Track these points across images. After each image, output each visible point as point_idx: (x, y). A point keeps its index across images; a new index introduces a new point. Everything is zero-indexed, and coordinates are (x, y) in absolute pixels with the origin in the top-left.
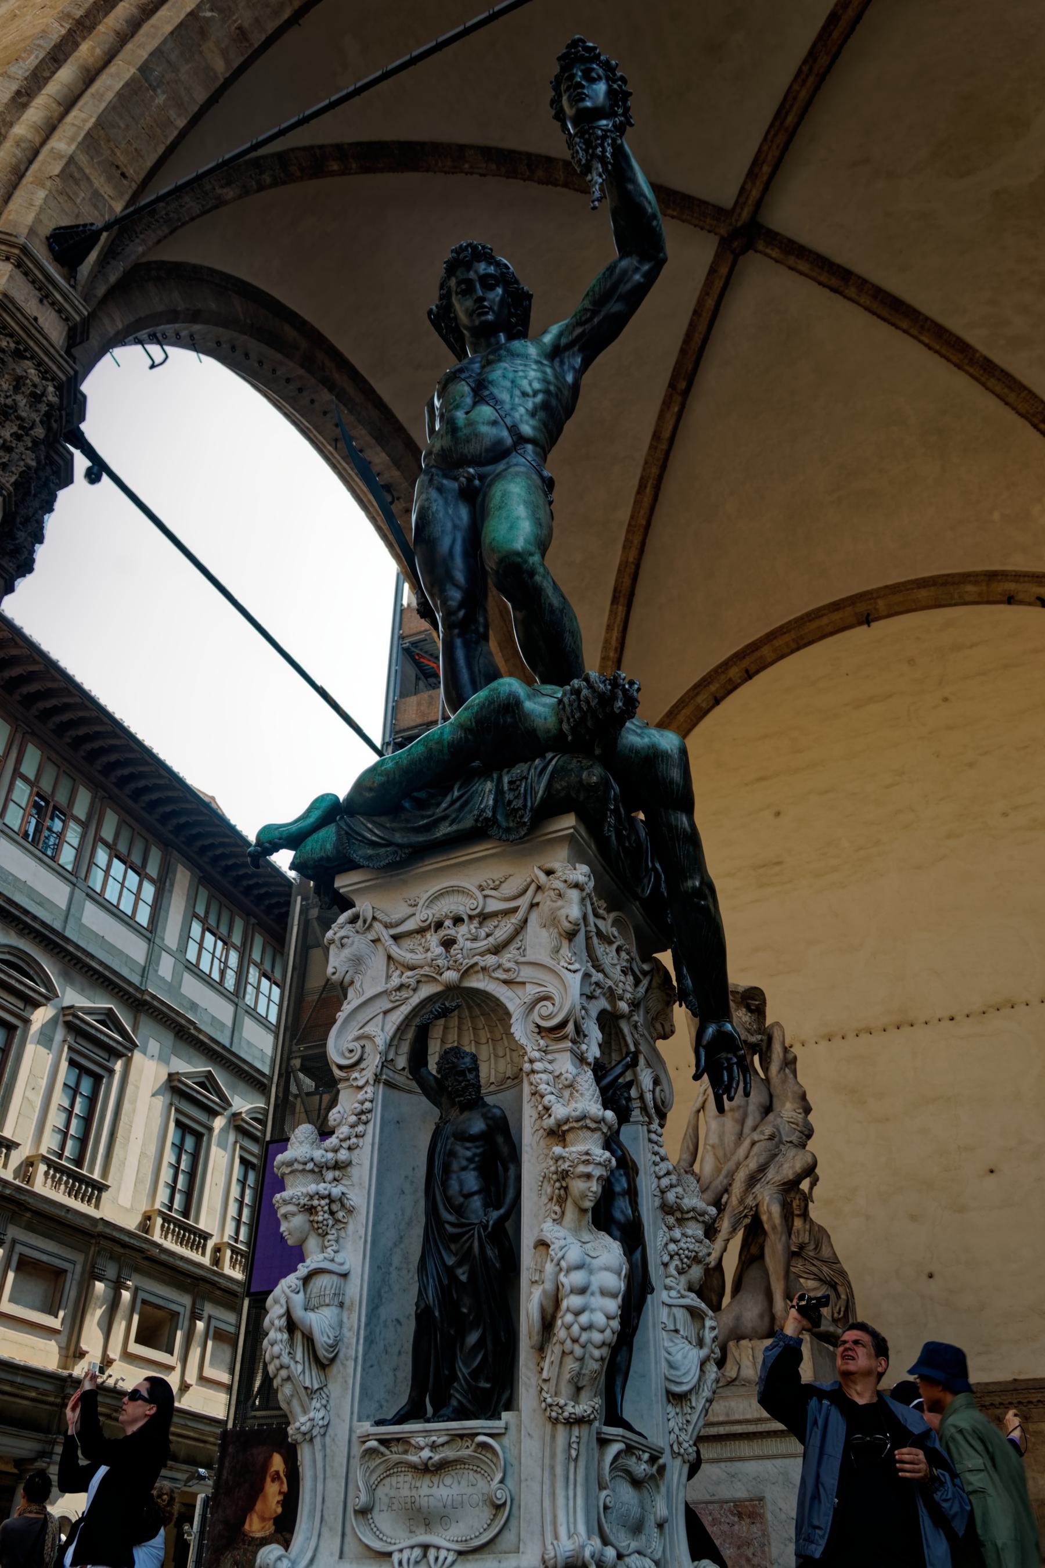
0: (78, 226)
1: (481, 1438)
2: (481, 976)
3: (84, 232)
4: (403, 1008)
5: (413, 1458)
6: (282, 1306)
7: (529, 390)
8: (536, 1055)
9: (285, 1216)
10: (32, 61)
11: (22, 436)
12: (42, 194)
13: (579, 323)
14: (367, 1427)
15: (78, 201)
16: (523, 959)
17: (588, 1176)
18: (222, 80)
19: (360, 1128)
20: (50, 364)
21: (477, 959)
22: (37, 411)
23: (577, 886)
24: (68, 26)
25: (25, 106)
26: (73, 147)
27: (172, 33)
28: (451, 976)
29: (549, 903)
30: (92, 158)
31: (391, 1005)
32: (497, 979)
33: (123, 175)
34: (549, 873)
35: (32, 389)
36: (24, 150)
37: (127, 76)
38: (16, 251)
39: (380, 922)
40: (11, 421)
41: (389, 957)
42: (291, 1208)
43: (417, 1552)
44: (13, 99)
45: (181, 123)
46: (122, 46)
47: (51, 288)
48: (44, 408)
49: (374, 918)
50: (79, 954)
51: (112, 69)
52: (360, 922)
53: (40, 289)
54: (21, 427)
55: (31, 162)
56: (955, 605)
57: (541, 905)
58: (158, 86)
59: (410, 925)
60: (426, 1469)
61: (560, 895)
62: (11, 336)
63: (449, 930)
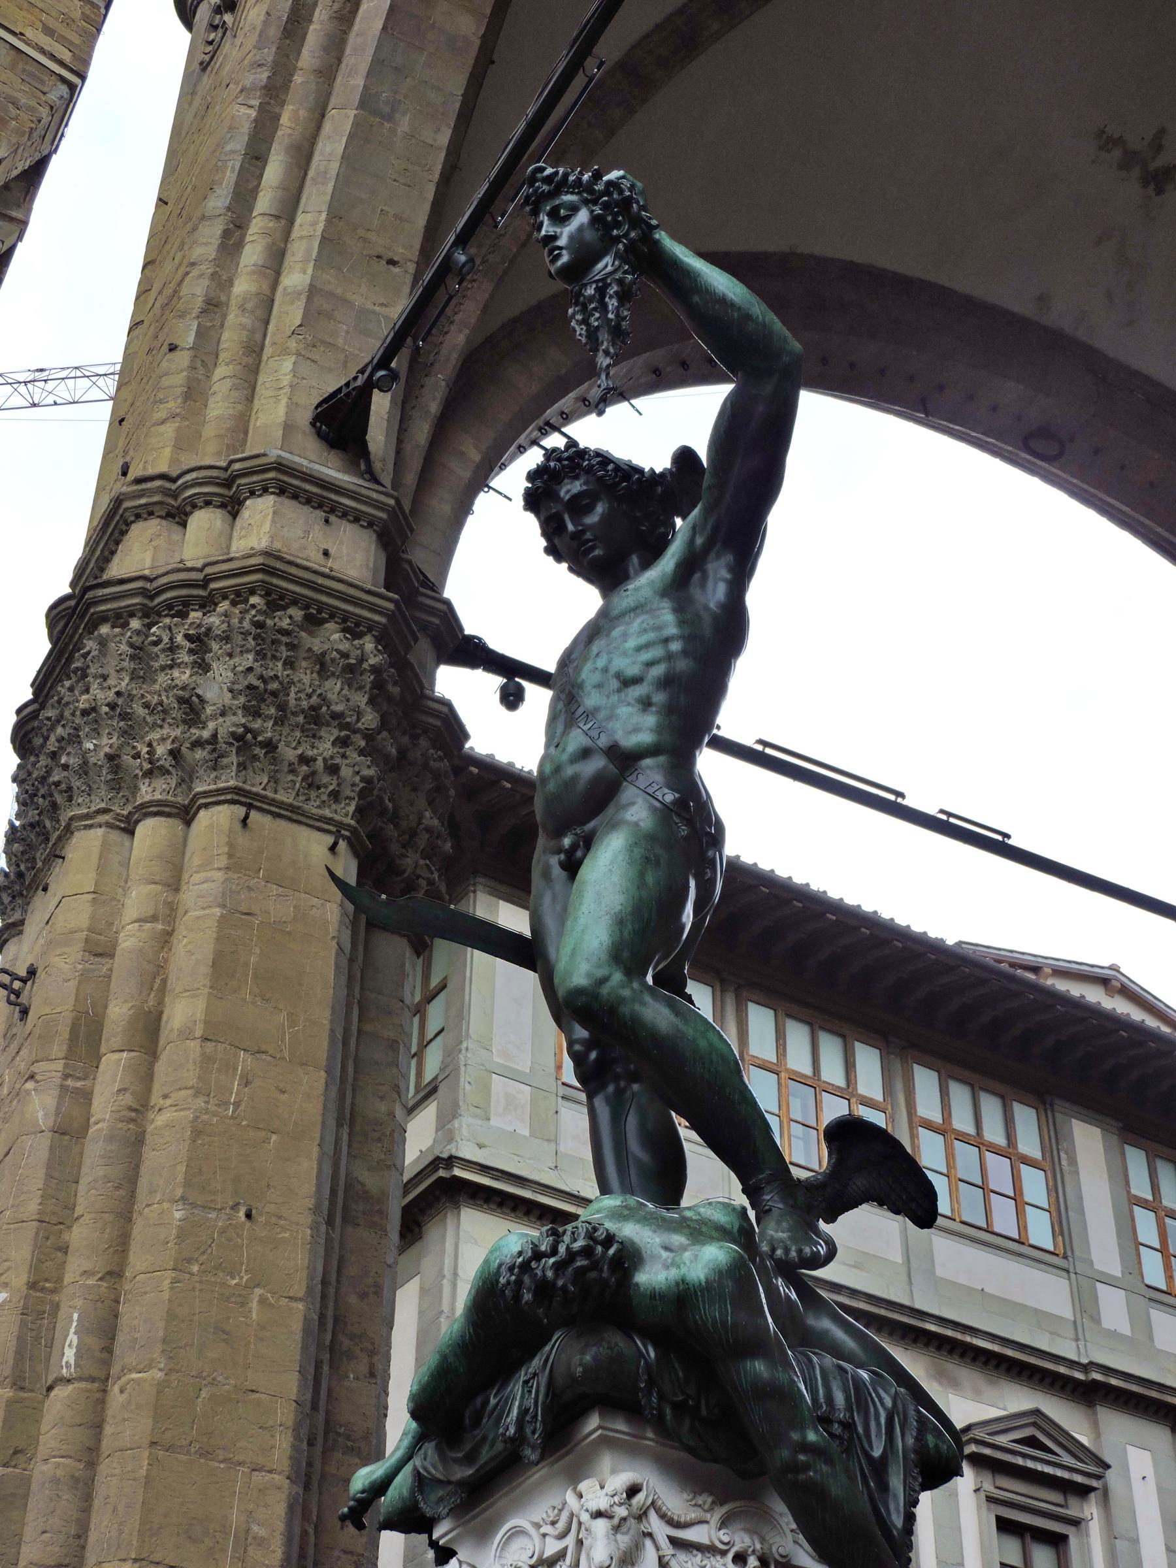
0: (339, 390)
3: (348, 395)
7: (633, 671)
10: (230, 177)
11: (348, 737)
12: (288, 364)
15: (340, 342)
18: (478, 42)
20: (358, 611)
22: (360, 688)
23: (599, 1514)
24: (256, 103)
25: (239, 245)
26: (310, 271)
27: (384, 28)
30: (340, 269)
33: (391, 262)
35: (343, 662)
36: (253, 312)
37: (348, 127)
38: (271, 475)
40: (328, 725)
44: (223, 247)
45: (444, 137)
46: (331, 85)
47: (333, 496)
48: (369, 679)
50: (949, 1333)
51: (327, 127)
53: (320, 506)
54: (342, 727)
55: (267, 323)
58: (394, 110)
62: (294, 603)
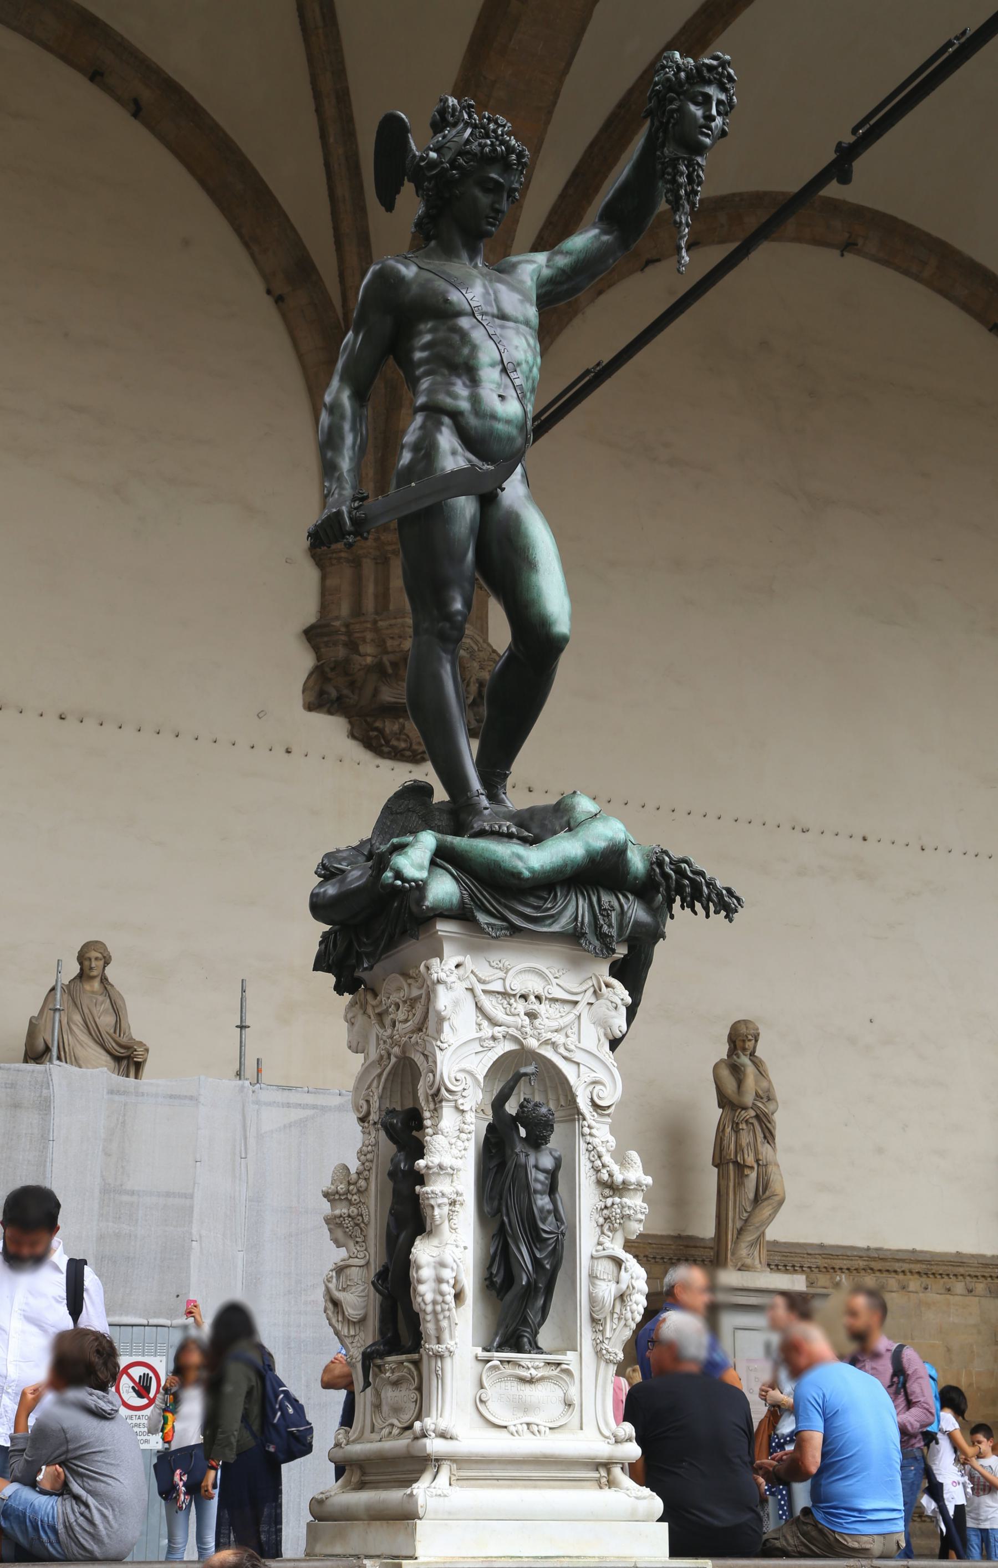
1: (564, 1366)
2: (549, 1047)
4: (490, 1053)
5: (525, 1374)
6: (452, 1269)
8: (593, 1124)
9: (439, 1206)
13: (551, 281)
14: (479, 1351)
16: (579, 1045)
17: (640, 1221)
19: (466, 1143)
21: (549, 1035)
28: (532, 1043)
29: (604, 1009)
31: (481, 1049)
32: (560, 1054)
34: (607, 986)
39: (476, 976)
41: (479, 1008)
42: (445, 1200)
43: (525, 1426)
49: (472, 972)
52: (461, 970)
56: (15, 29)
57: (594, 1006)
59: (497, 986)
60: (531, 1381)
61: (616, 1008)
63: (534, 1006)
